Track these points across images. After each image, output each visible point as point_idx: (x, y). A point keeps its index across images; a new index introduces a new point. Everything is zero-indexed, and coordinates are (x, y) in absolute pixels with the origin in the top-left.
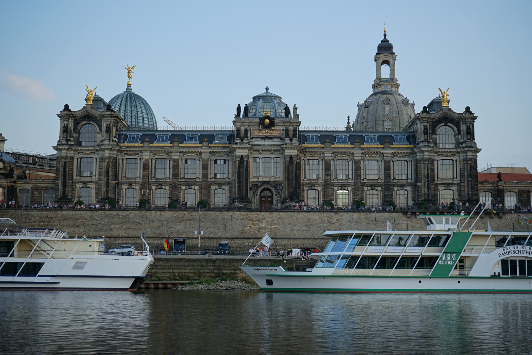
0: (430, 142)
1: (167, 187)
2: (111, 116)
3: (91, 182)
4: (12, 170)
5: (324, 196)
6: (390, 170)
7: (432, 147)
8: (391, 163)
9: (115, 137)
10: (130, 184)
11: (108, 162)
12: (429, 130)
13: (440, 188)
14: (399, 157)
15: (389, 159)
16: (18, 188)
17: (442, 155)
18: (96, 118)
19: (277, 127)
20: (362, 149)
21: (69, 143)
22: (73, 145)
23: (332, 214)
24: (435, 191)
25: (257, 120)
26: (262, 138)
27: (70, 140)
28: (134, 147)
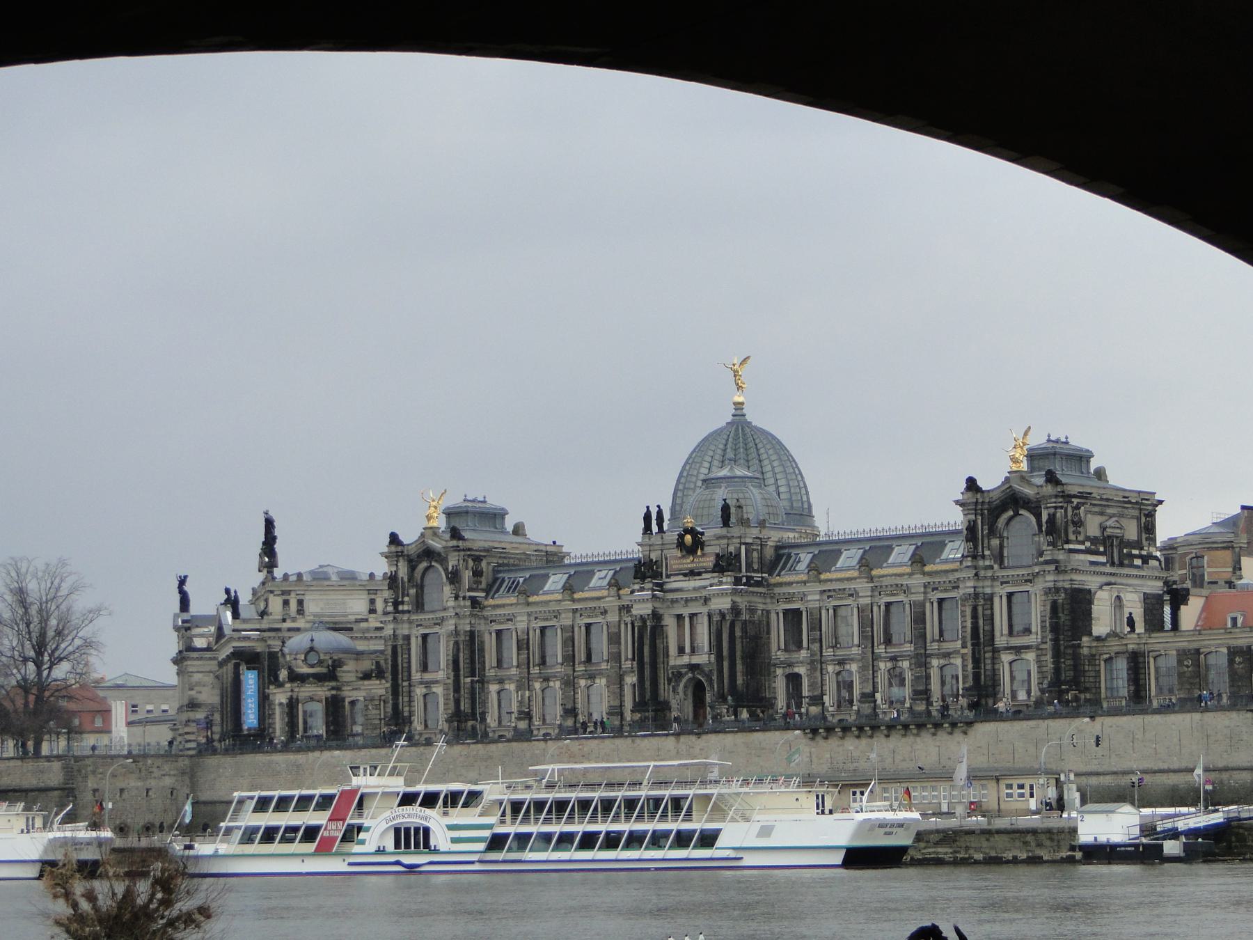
0: (983, 557)
1: (558, 684)
2: (457, 549)
3: (437, 682)
4: (337, 664)
5: (812, 686)
6: (924, 622)
7: (991, 567)
8: (928, 605)
9: (470, 589)
10: (501, 682)
11: (456, 643)
12: (982, 530)
13: (1006, 658)
15: (921, 597)
16: (347, 700)
18: (439, 554)
19: (708, 550)
20: (871, 579)
21: (400, 608)
22: (409, 612)
23: (693, 738)
24: (993, 664)
25: (672, 537)
26: (685, 575)
27: (402, 603)
28: (503, 606)
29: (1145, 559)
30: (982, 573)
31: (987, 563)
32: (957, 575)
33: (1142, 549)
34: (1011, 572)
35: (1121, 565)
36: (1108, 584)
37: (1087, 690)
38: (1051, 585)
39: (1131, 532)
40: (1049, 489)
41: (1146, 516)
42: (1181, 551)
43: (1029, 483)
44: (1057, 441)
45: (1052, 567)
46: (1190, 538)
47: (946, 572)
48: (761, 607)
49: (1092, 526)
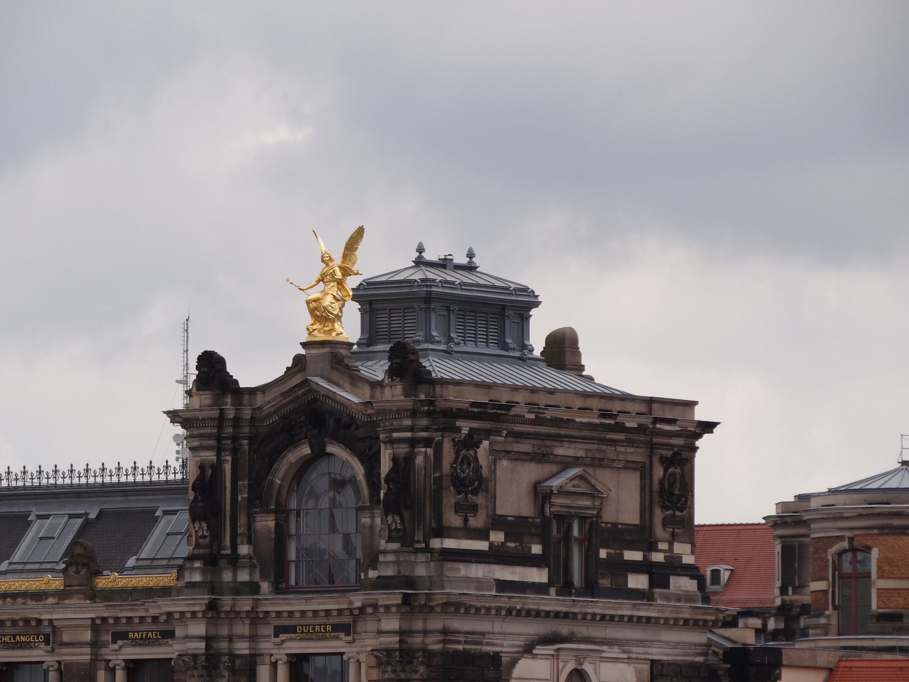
7: (253, 588)
14: (136, 643)
17: (291, 629)
29: (660, 575)
30: (227, 601)
31: (244, 576)
32: (165, 606)
33: (652, 547)
34: (296, 604)
35: (591, 589)
36: (547, 640)
38: (392, 641)
39: (623, 501)
40: (395, 394)
41: (667, 462)
42: (818, 531)
43: (355, 379)
44: (444, 264)
45: (394, 598)
46: (838, 499)
47: (150, 593)
49: (514, 490)
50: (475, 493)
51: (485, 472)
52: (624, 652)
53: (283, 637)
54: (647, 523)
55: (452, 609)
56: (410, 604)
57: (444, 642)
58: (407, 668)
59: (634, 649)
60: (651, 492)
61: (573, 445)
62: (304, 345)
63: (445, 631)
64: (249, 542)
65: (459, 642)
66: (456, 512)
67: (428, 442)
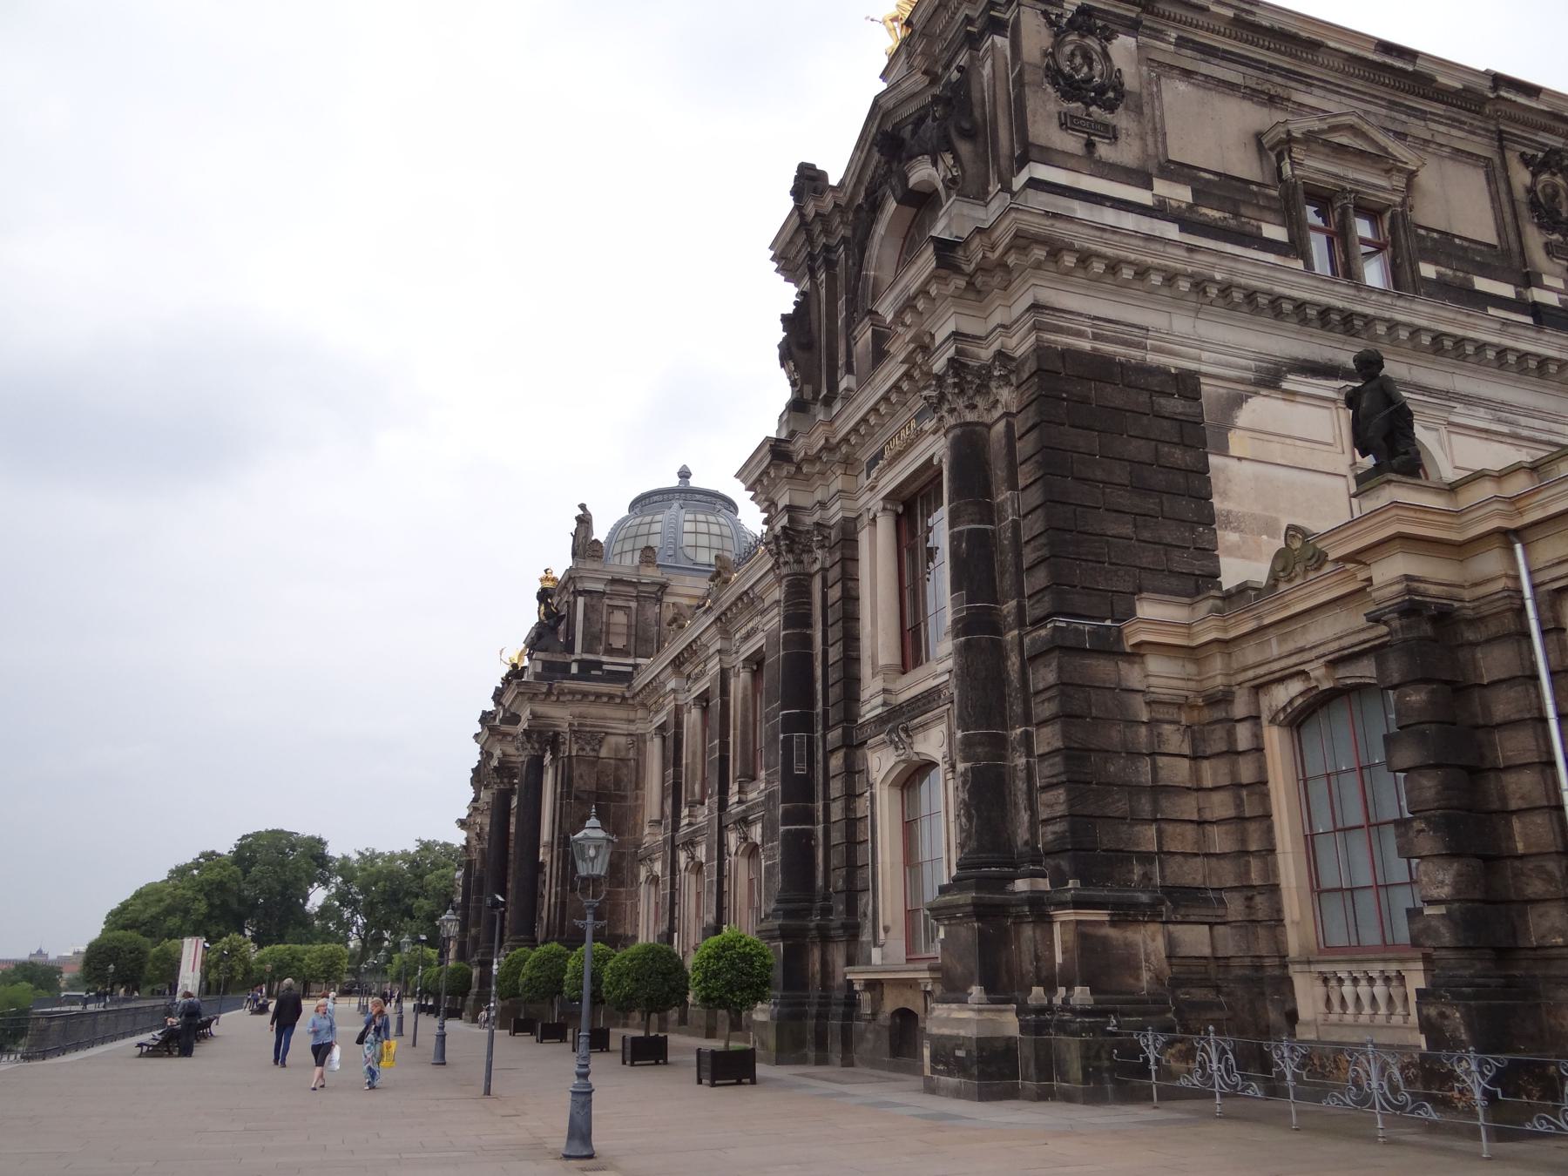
33: (1530, 279)
37: (1184, 900)
48: (624, 727)
50: (1111, 107)
51: (1130, 82)
52: (1499, 421)
53: (874, 474)
54: (1515, 246)
55: (1039, 253)
56: (958, 270)
57: (1037, 327)
58: (980, 402)
59: (1523, 421)
60: (1512, 202)
61: (1336, 98)
62: (884, 76)
63: (1036, 307)
64: (849, 370)
65: (1080, 334)
66: (1063, 125)
67: (997, 26)
